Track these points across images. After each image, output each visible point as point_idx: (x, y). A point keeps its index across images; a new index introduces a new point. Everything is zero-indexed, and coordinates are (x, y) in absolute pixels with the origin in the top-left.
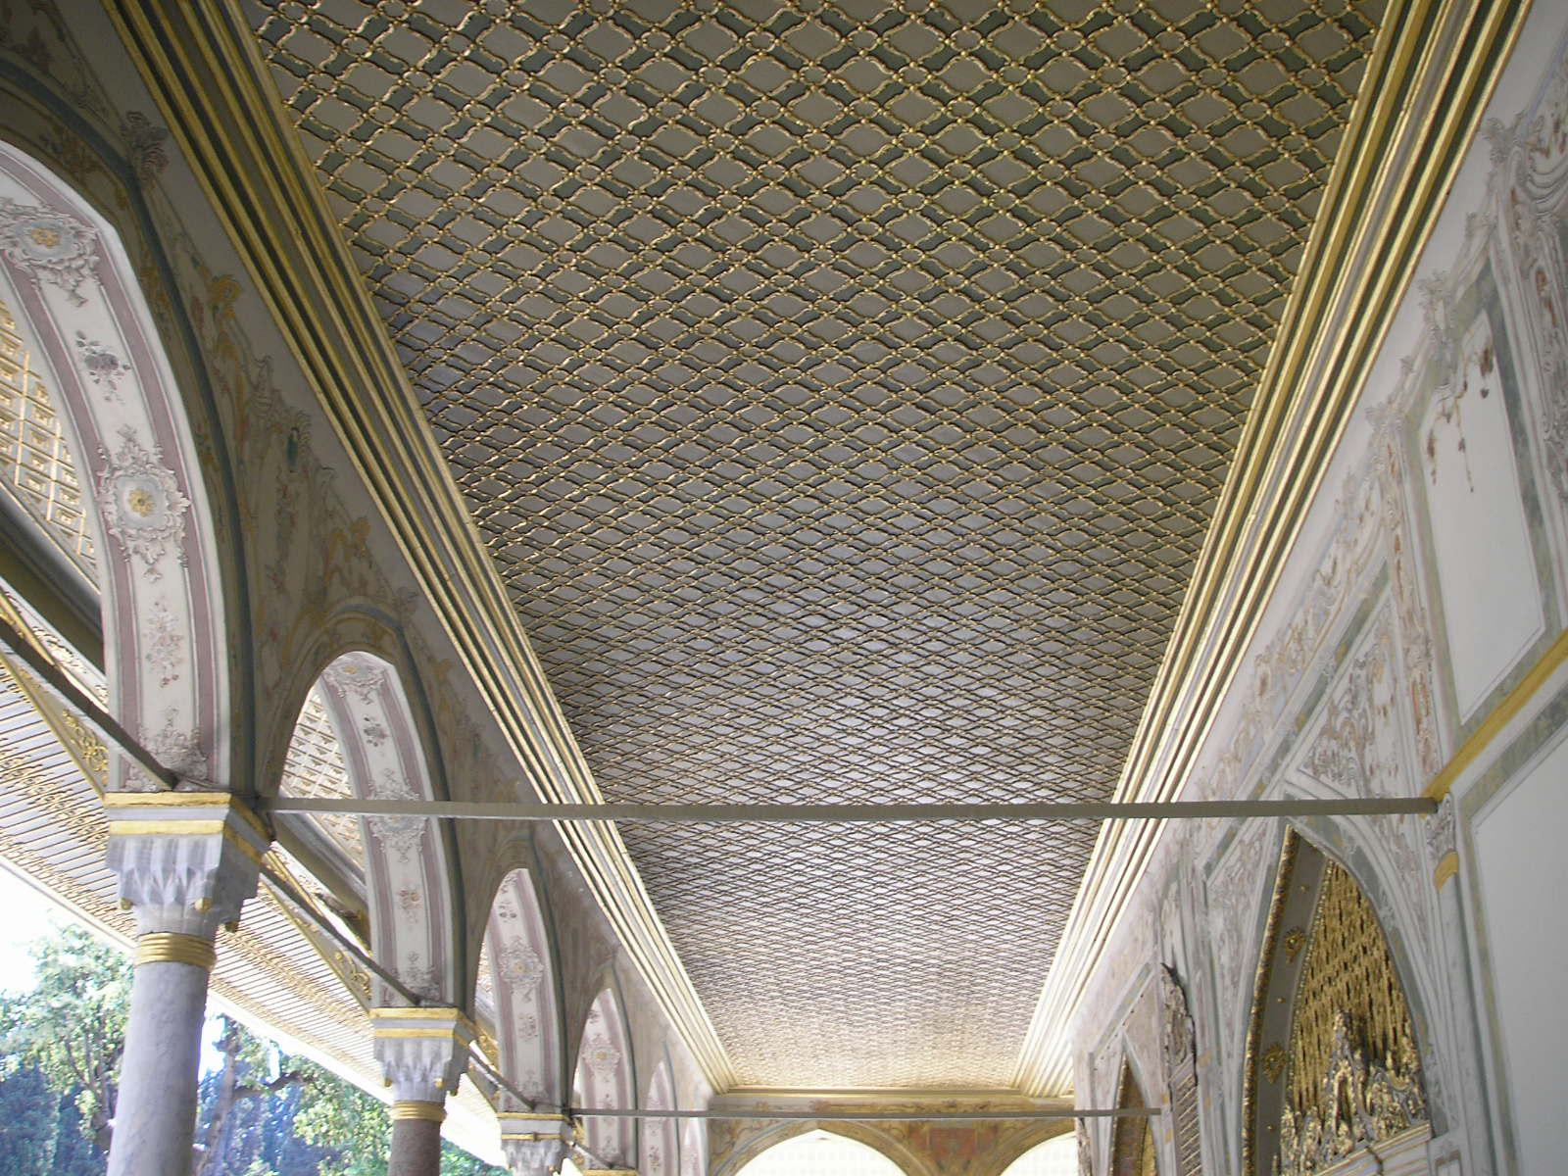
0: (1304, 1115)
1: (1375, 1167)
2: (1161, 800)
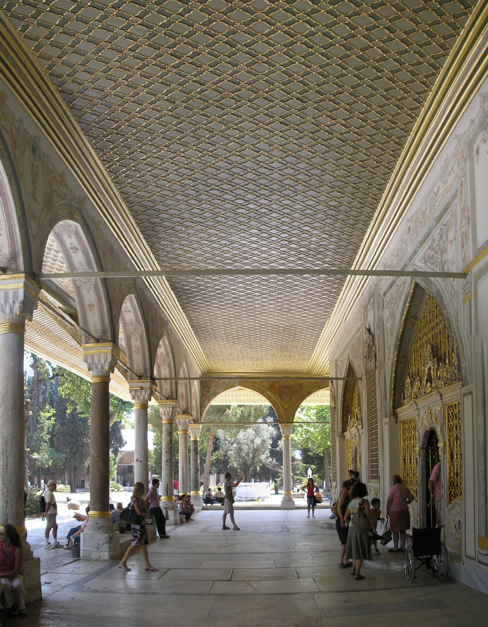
0: (414, 380)
1: (439, 397)
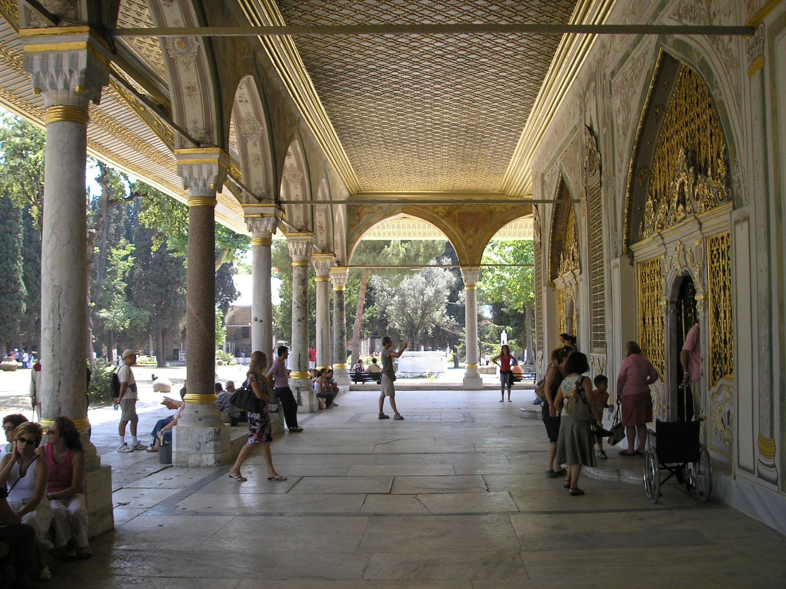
0: (659, 201)
1: (698, 226)
2: (590, 35)
